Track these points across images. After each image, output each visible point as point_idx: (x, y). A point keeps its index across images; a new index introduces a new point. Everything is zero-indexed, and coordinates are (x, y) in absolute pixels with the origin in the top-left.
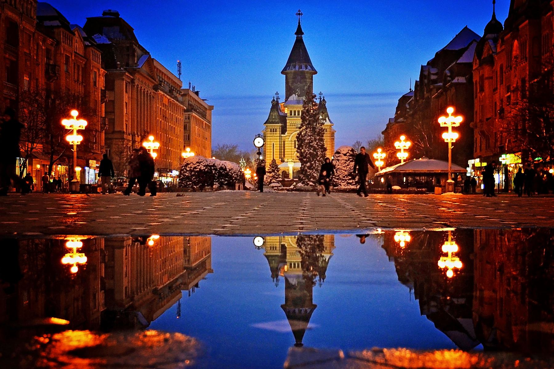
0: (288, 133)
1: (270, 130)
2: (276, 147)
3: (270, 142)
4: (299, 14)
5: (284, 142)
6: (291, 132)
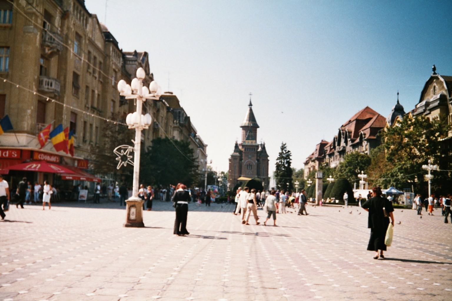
4: (250, 95)
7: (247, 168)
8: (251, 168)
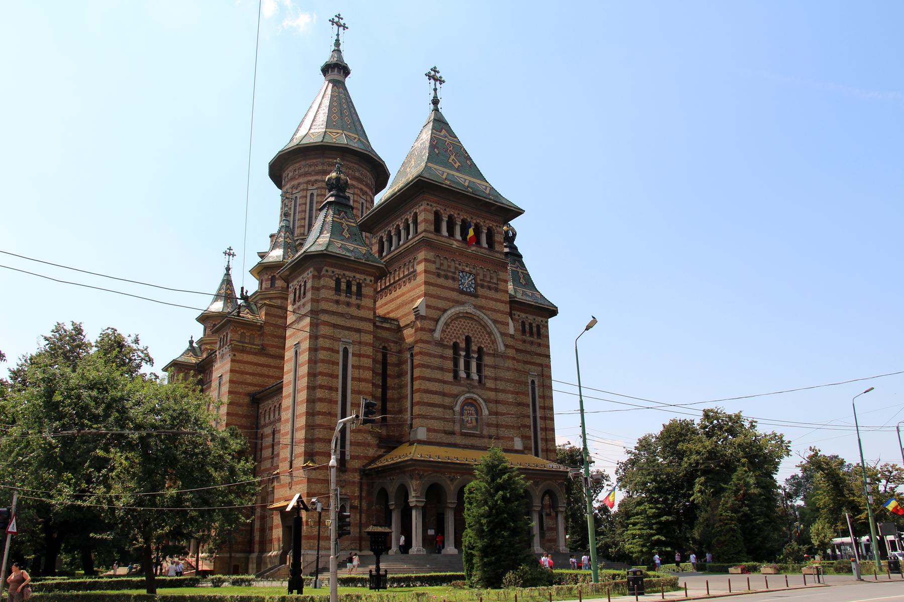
1: (332, 284)
6: (441, 304)
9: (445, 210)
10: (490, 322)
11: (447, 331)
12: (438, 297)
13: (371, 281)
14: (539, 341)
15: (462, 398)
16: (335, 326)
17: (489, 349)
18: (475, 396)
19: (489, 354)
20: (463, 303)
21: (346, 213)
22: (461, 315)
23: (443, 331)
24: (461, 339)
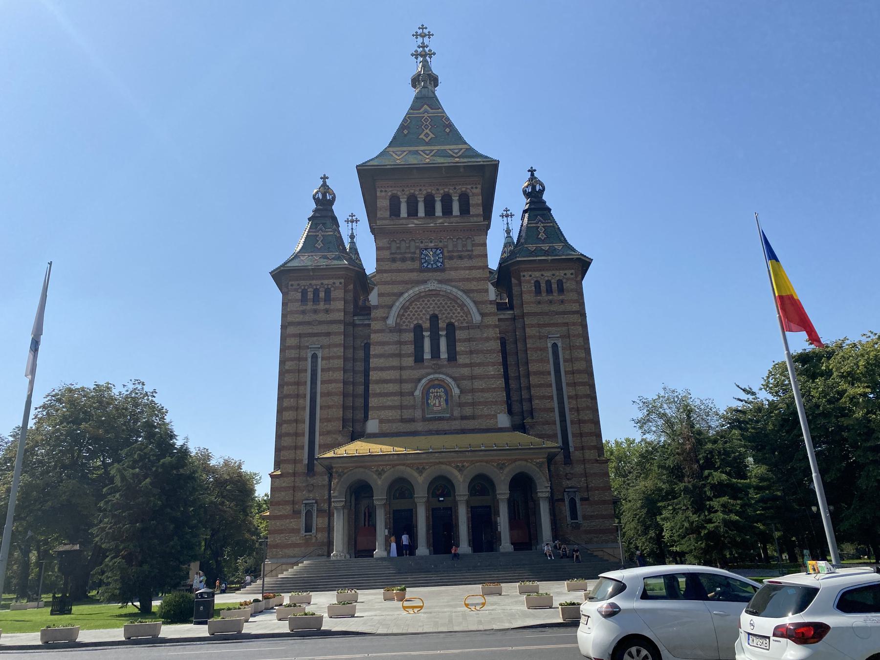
0: (380, 295)
1: (299, 296)
2: (329, 369)
3: (299, 347)
5: (367, 347)
6: (396, 289)
7: (419, 358)
8: (452, 356)
9: (403, 191)
10: (460, 294)
11: (406, 314)
12: (393, 283)
13: (341, 283)
14: (561, 297)
15: (424, 381)
16: (300, 336)
17: (462, 323)
18: (441, 376)
19: (461, 328)
20: (425, 282)
21: (324, 224)
22: (422, 294)
23: (400, 316)
24: (424, 319)
